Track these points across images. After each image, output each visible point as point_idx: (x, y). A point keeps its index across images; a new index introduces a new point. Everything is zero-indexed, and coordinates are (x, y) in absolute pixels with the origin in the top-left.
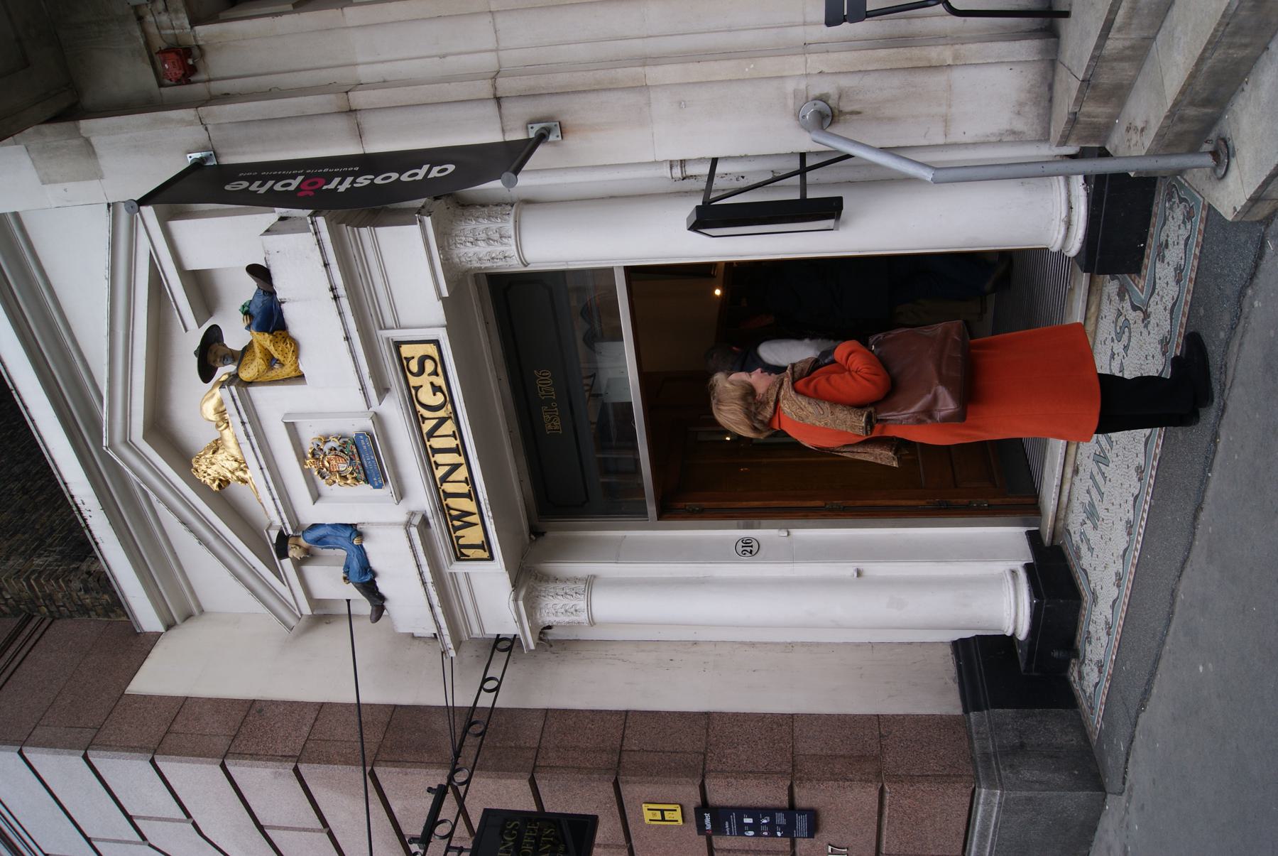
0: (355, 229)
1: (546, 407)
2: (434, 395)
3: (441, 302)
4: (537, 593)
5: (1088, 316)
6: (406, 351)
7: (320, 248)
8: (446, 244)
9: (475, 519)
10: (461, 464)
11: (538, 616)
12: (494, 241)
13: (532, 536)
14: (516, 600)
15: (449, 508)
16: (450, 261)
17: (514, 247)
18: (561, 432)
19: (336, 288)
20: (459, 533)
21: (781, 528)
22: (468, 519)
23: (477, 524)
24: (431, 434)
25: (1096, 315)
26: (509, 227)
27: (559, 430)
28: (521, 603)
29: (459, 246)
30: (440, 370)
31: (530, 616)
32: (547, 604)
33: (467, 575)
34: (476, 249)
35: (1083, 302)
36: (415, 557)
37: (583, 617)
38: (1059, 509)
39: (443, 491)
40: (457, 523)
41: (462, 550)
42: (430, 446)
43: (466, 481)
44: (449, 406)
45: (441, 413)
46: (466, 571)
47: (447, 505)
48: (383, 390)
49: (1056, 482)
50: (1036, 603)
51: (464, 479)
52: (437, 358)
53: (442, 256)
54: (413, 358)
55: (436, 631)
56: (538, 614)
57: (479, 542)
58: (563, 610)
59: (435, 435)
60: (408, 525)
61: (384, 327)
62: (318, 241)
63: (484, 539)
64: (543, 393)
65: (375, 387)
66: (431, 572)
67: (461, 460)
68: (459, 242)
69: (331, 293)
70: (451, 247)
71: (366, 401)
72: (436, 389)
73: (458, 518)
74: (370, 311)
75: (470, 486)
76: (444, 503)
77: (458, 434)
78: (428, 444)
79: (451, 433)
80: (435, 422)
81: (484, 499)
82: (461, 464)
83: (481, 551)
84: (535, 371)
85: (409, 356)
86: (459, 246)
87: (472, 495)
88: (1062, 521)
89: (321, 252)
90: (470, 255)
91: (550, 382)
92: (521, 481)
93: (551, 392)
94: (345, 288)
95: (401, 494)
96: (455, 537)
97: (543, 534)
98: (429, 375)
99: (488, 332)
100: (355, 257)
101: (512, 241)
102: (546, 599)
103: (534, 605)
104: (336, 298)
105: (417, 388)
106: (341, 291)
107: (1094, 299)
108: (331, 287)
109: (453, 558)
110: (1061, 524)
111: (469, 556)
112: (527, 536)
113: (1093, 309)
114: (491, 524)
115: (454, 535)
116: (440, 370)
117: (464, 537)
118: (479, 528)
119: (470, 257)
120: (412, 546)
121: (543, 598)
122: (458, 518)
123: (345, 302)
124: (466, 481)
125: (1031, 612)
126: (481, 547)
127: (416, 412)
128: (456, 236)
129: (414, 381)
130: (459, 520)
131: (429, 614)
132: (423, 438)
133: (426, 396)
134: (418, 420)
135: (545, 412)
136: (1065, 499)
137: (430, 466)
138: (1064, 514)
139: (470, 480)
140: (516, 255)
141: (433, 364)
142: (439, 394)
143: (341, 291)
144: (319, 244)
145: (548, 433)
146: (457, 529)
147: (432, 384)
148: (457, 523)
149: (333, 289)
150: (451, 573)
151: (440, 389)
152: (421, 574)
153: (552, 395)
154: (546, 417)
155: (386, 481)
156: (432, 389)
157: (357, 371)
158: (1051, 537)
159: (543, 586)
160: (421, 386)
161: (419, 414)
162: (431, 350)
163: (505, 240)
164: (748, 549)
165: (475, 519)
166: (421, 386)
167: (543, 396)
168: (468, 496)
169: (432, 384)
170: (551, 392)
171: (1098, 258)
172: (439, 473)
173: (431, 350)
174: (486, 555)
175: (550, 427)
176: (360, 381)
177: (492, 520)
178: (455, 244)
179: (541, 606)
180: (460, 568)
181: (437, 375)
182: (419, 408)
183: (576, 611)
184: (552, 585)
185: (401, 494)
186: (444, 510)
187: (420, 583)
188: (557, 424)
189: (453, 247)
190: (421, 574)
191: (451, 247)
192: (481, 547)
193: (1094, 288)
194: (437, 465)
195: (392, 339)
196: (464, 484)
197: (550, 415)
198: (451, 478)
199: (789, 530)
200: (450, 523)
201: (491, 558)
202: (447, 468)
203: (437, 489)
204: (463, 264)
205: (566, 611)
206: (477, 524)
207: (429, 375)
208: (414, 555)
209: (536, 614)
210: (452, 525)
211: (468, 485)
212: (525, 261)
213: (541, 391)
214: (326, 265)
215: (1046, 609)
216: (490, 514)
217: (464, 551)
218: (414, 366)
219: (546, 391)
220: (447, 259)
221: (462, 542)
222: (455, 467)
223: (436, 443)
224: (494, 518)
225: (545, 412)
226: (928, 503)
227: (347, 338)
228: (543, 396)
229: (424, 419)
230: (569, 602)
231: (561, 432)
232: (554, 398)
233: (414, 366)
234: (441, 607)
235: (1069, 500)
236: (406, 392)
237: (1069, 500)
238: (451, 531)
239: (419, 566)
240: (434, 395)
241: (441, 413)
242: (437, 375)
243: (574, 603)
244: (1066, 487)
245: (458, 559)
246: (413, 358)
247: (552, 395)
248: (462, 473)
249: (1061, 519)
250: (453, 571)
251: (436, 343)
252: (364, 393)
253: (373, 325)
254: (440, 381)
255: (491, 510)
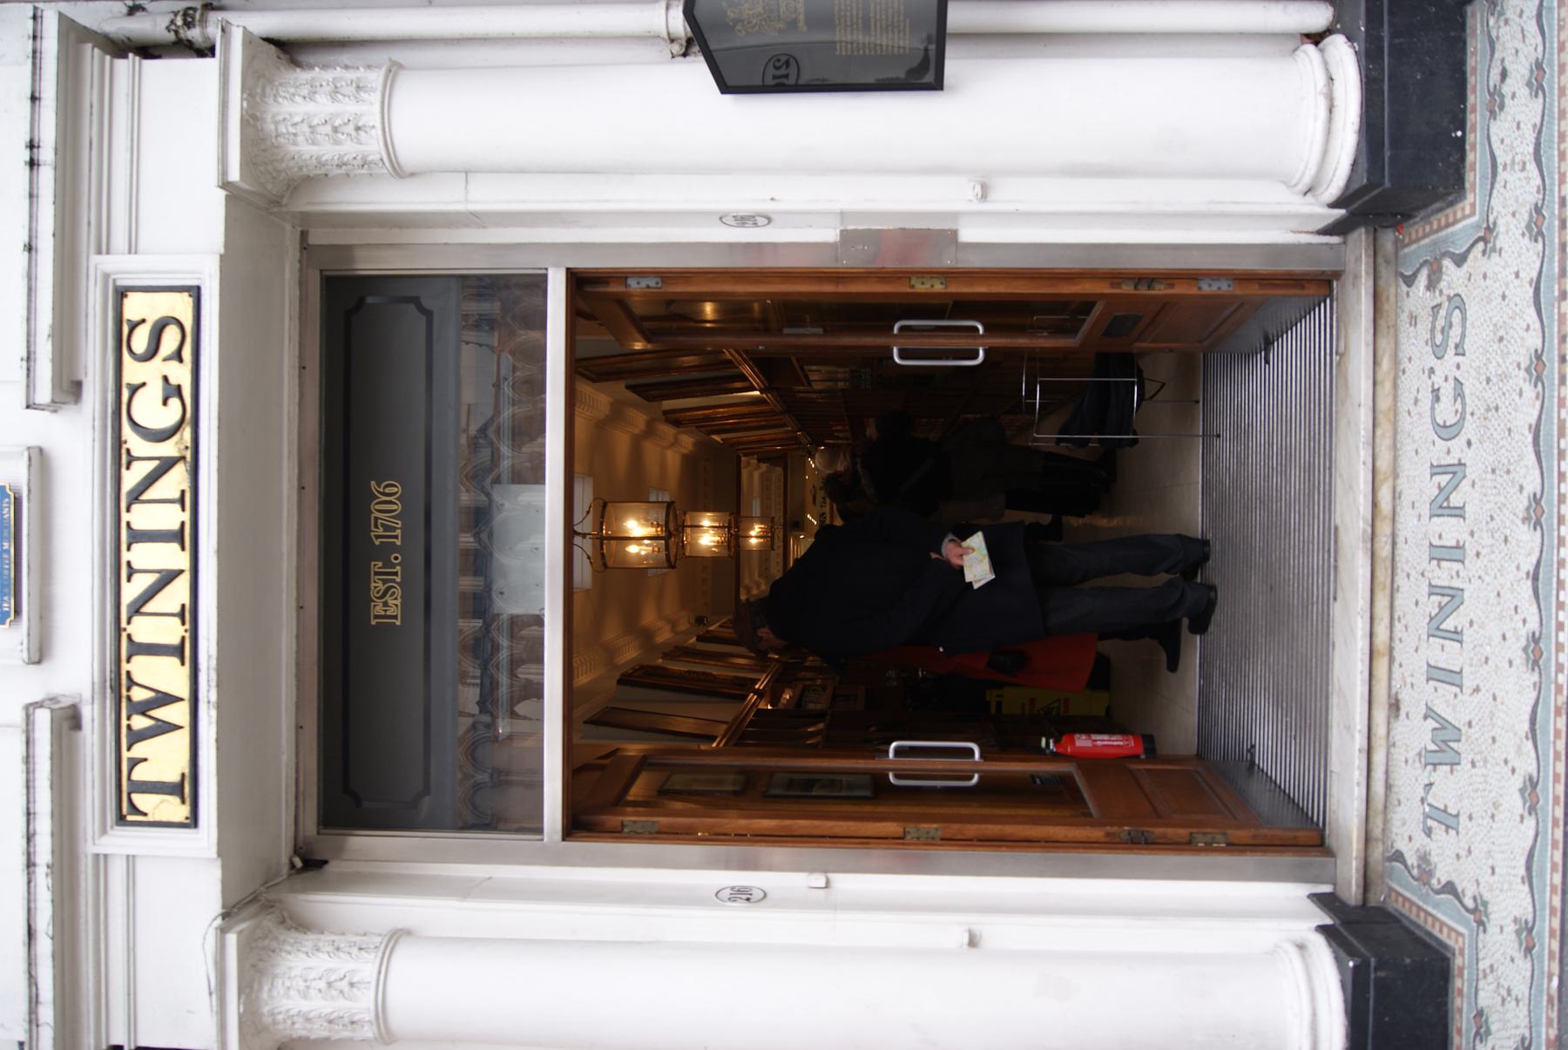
0: (108, 58)
1: (380, 564)
2: (165, 403)
3: (222, 194)
4: (274, 944)
5: (1380, 377)
6: (134, 307)
7: (34, 64)
8: (259, 90)
9: (177, 713)
10: (182, 572)
11: (265, 995)
12: (344, 95)
13: (298, 863)
14: (223, 931)
15: (132, 683)
16: (259, 124)
17: (377, 108)
18: (398, 623)
19: (39, 147)
20: (139, 750)
21: (813, 870)
22: (163, 713)
23: (181, 727)
24: (136, 496)
25: (1392, 376)
26: (375, 78)
27: (395, 617)
28: (232, 939)
29: (280, 100)
30: (187, 353)
31: (248, 987)
32: (290, 968)
33: (131, 860)
34: (310, 107)
35: (1367, 345)
36: (28, 787)
37: (362, 1004)
38: (1371, 813)
39: (129, 636)
40: (139, 722)
41: (135, 797)
42: (128, 524)
43: (181, 615)
44: (187, 433)
45: (169, 449)
46: (131, 852)
47: (128, 673)
48: (70, 389)
49: (1359, 741)
50: (1355, 967)
51: (177, 609)
52: (188, 325)
53: (245, 104)
54: (143, 321)
55: (23, 1037)
56: (266, 988)
57: (174, 777)
58: (322, 984)
59: (144, 497)
60: (30, 709)
61: (103, 248)
62: (34, 52)
63: (187, 771)
64: (380, 531)
65: (53, 360)
66: (53, 835)
67: (180, 560)
68: (283, 94)
69: (27, 153)
70: (266, 100)
71: (28, 386)
72: (171, 391)
73: (143, 708)
74: (87, 215)
75: (187, 626)
76: (125, 667)
77: (190, 499)
78: (125, 517)
79: (177, 495)
80: (153, 465)
81: (209, 657)
82: (182, 572)
83: (175, 800)
84: (373, 483)
85: (136, 318)
86: (280, 100)
87: (186, 651)
88: (1380, 845)
89: (34, 73)
90: (297, 119)
91: (398, 507)
92: (299, 727)
93: (394, 529)
94: (56, 149)
95: (40, 653)
96: (130, 759)
97: (322, 863)
98: (165, 360)
99: (301, 385)
100: (91, 106)
101: (376, 98)
102: (289, 957)
103: (261, 965)
104: (33, 164)
105: (134, 389)
106: (47, 154)
107: (1385, 345)
108: (31, 141)
109: (111, 816)
110: (1377, 852)
111: (145, 814)
112: (285, 860)
113: (1385, 364)
114: (210, 723)
115: (125, 755)
116: (187, 353)
117: (145, 760)
118: (183, 737)
119: (295, 125)
120: (28, 759)
121: (284, 954)
122: (143, 708)
123: (46, 176)
124: (181, 615)
125: (1345, 1001)
126: (175, 789)
127: (119, 442)
128: (281, 84)
129: (133, 372)
130: (144, 714)
131: (21, 951)
132: (119, 500)
133: (152, 410)
134: (119, 457)
135: (377, 573)
136: (1379, 787)
137: (118, 571)
138: (1381, 825)
139: (189, 615)
140: (378, 125)
141: (178, 337)
142: (174, 403)
143: (47, 154)
144: (34, 57)
145: (373, 622)
146: (137, 737)
147: (166, 379)
148: (139, 722)
149: (32, 146)
150: (97, 856)
151: (178, 391)
152: (30, 837)
153: (396, 537)
154: (377, 585)
155: (18, 612)
156: (164, 389)
157: (28, 319)
158: (1361, 883)
159: (293, 936)
160: (144, 384)
161: (124, 447)
162: (181, 307)
163: (364, 95)
164: (743, 895)
165: (177, 713)
166: (144, 384)
167: (378, 537)
168: (178, 651)
169: (166, 379)
170: (394, 529)
171: (1387, 154)
172: (130, 592)
173: (181, 307)
174: (178, 811)
175: (378, 609)
176: (28, 342)
177: (214, 713)
178: (275, 96)
179: (278, 971)
180: (120, 842)
181: (181, 360)
182: (127, 431)
183: (352, 985)
184: (311, 936)
185: (40, 653)
186: (117, 684)
187: (21, 860)
188: (394, 604)
189: (270, 100)
190: (30, 837)
191: (266, 100)
192: (175, 789)
193: (1382, 323)
194: (132, 572)
195: (114, 280)
196: (177, 621)
197: (385, 582)
198: (150, 607)
199: (831, 875)
200: (124, 722)
201: (193, 821)
202: (150, 579)
203: (119, 630)
204: (281, 140)
205: (330, 985)
206: (181, 727)
207: (165, 360)
208: (28, 781)
209: (260, 989)
210: (129, 727)
211: (183, 623)
212: (398, 163)
213: (376, 527)
214: (34, 99)
215: (1377, 980)
216: (213, 697)
217: (139, 799)
218: (140, 341)
219: (386, 528)
220: (255, 118)
221: (140, 774)
222: (168, 577)
223: (141, 517)
224: (220, 707)
225: (377, 573)
226: (1108, 835)
227: (30, 248)
228: (378, 537)
229: (131, 459)
230: (341, 965)
231: (398, 623)
232: (398, 542)
233: (140, 341)
234: (52, 938)
235: (1388, 787)
236: (111, 396)
237: (1388, 787)
238: (123, 738)
239: (29, 815)
240: (165, 403)
241: (169, 449)
242: (181, 360)
243: (352, 966)
244: (1379, 758)
245: (121, 820)
246: (143, 321)
247: (396, 537)
248: (177, 594)
249: (1377, 840)
250: (101, 850)
251: (196, 293)
252: (28, 369)
253: (87, 238)
254: (181, 374)
255: (218, 686)
